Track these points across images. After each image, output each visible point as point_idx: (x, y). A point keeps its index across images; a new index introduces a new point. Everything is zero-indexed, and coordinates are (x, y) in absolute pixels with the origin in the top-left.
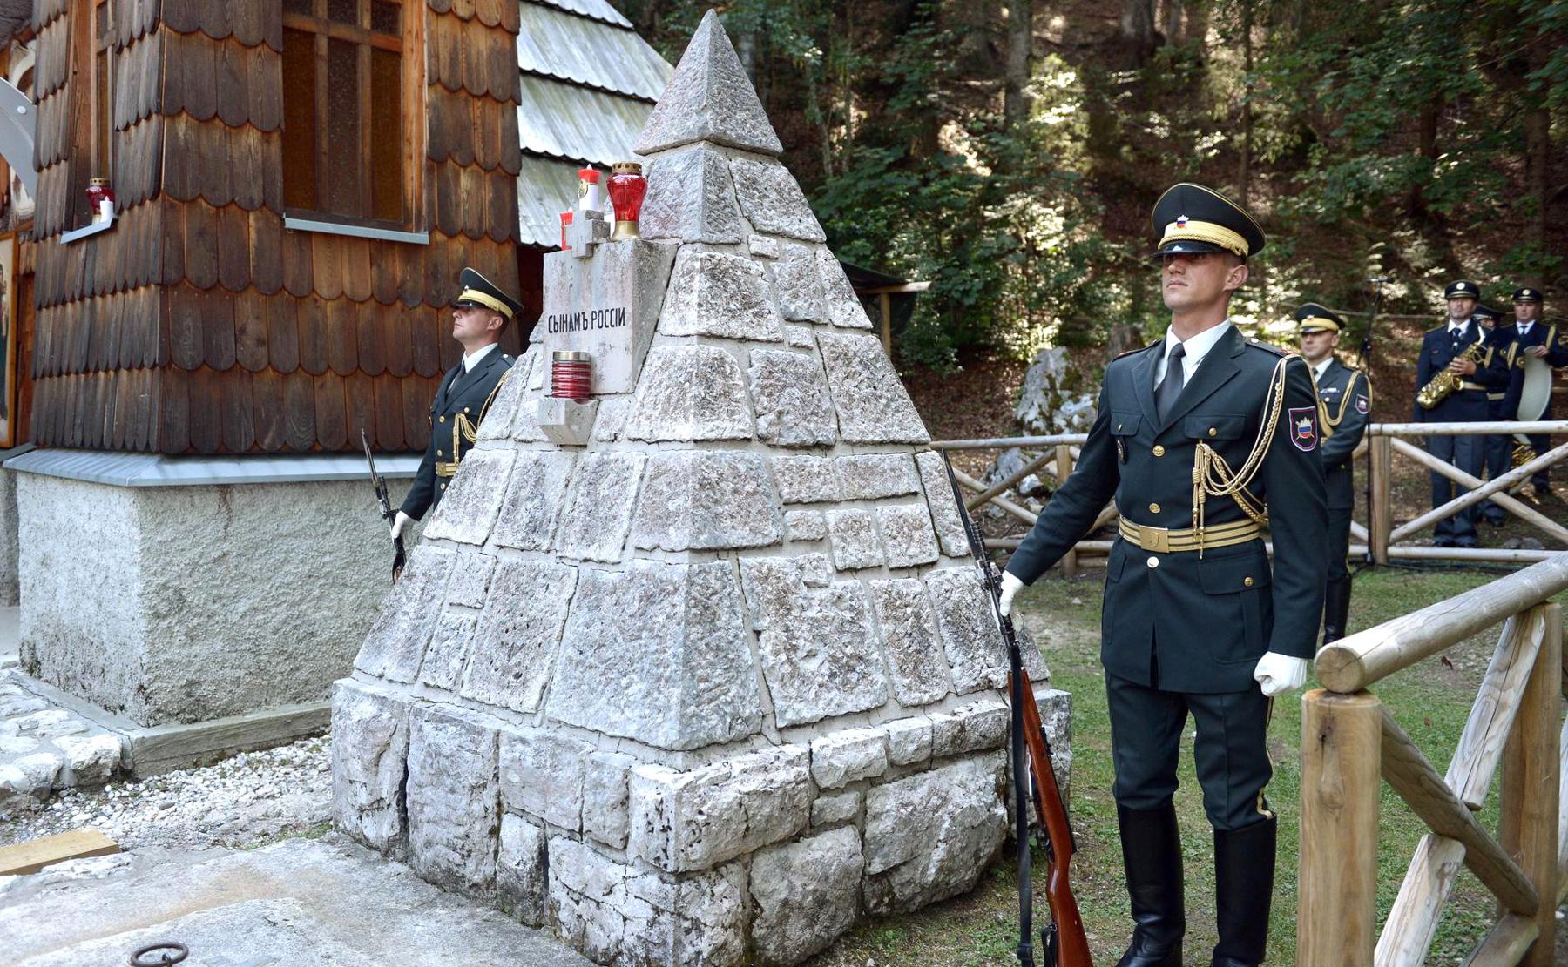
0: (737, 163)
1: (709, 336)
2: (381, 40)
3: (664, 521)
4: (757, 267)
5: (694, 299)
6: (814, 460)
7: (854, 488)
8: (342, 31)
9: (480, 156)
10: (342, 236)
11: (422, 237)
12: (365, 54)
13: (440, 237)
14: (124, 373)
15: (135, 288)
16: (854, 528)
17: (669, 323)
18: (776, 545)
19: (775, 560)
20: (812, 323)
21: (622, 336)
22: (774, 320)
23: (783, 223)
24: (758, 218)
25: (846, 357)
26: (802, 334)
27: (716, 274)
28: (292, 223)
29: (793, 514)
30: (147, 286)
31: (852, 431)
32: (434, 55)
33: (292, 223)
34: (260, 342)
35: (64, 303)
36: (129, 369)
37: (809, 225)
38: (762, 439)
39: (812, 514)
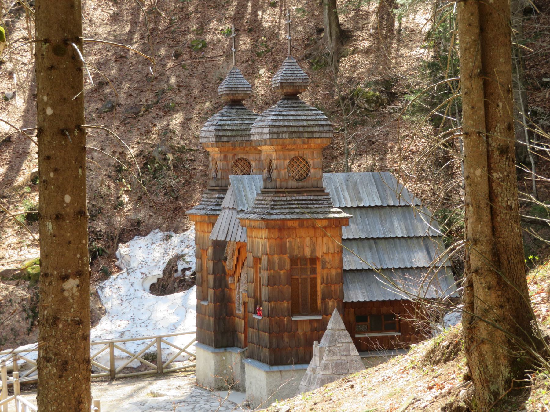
0: (337, 332)
1: (327, 360)
2: (312, 276)
8: (304, 276)
9: (334, 297)
10: (304, 320)
11: (320, 317)
12: (309, 280)
13: (325, 316)
21: (318, 359)
24: (339, 341)
25: (352, 360)
26: (344, 358)
27: (330, 351)
28: (294, 319)
32: (323, 278)
33: (294, 319)
34: (287, 343)
38: (334, 374)
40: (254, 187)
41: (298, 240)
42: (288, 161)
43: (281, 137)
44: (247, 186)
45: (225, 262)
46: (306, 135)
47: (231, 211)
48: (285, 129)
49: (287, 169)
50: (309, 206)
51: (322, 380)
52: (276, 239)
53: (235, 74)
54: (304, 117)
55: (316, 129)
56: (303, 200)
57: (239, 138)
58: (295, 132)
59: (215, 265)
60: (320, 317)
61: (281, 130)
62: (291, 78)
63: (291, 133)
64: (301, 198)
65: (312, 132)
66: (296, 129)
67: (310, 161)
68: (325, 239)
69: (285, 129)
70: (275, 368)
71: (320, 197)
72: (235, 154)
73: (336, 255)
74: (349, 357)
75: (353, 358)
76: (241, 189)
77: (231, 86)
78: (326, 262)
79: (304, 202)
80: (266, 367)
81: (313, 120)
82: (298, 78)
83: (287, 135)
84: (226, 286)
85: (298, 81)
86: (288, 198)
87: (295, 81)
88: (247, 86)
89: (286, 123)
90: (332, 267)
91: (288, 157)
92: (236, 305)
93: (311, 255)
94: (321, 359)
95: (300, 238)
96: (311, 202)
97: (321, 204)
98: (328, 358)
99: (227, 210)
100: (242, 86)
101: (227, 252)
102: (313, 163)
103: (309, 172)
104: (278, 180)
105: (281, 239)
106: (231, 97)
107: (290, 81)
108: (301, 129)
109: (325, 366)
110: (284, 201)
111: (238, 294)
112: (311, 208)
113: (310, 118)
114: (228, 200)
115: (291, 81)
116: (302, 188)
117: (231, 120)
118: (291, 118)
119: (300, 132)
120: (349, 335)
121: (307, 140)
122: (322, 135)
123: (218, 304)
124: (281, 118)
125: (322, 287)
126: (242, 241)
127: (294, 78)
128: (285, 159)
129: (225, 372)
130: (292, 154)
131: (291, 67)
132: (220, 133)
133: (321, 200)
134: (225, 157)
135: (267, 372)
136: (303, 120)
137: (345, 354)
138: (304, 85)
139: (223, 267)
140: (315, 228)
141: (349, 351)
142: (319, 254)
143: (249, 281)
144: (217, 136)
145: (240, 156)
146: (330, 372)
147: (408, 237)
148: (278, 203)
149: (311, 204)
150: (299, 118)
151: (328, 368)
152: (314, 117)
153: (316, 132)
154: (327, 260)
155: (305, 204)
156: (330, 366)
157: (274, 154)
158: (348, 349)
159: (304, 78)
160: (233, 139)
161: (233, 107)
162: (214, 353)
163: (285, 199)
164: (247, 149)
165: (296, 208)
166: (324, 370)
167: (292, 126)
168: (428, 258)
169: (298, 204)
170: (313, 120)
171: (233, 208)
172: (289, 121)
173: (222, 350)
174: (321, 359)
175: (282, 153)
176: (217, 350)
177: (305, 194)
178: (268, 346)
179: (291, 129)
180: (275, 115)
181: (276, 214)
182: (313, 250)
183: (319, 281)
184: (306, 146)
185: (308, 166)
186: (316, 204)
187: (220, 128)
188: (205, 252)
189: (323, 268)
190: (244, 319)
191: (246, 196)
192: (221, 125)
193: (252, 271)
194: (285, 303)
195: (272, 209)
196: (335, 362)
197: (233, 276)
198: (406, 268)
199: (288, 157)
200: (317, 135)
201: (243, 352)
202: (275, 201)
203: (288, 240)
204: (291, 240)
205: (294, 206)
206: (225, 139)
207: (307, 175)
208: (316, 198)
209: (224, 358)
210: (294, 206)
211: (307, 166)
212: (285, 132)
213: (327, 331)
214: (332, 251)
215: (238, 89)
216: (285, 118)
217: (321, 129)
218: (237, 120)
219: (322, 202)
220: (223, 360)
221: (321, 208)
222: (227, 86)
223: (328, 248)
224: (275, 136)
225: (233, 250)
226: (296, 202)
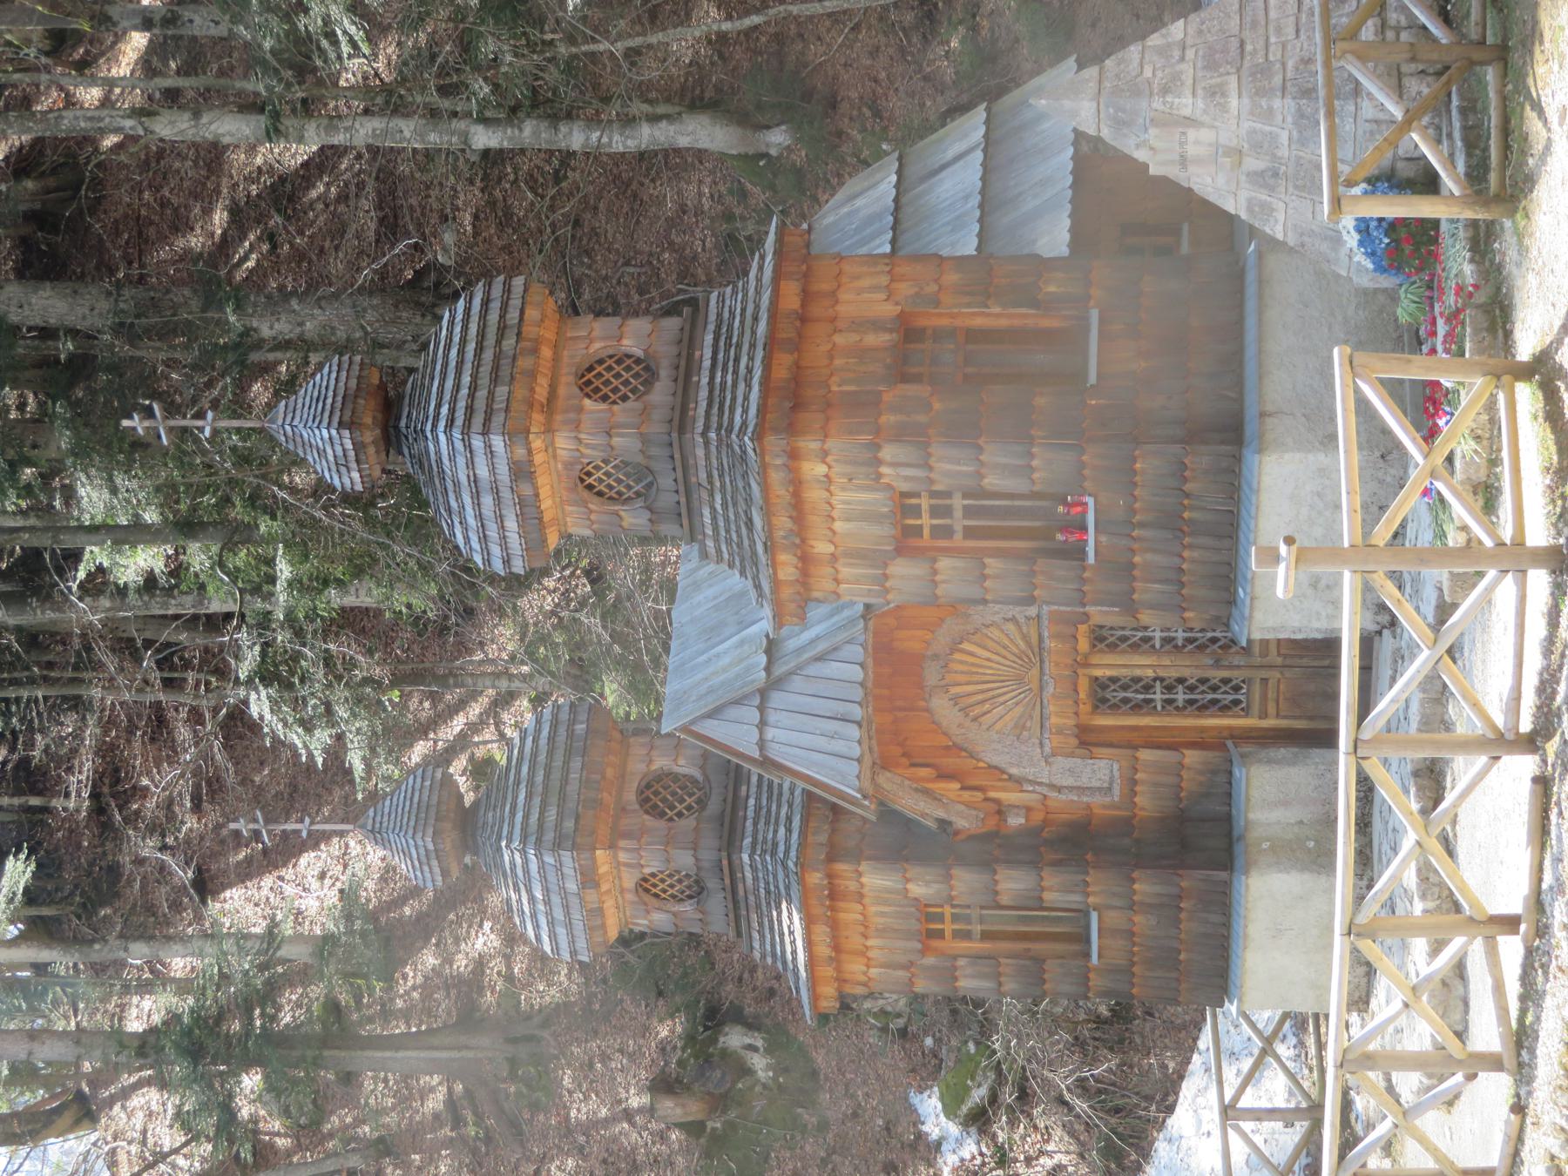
0: (1107, 84)
3: (1271, 110)
4: (1159, 74)
5: (1177, 101)
6: (1249, 48)
7: (1261, 31)
10: (1099, 356)
11: (1094, 315)
13: (1092, 303)
14: (1188, 487)
15: (1135, 472)
16: (1279, 30)
17: (1187, 112)
18: (1284, 65)
19: (1290, 64)
20: (1184, 49)
21: (1192, 134)
22: (1183, 66)
23: (1136, 63)
25: (1200, 32)
26: (1190, 54)
27: (1165, 91)
28: (1092, 378)
29: (1271, 58)
30: (1134, 460)
31: (1236, 31)
32: (969, 305)
33: (1092, 378)
35: (1133, 566)
36: (1185, 480)
37: (1134, 51)
39: (1272, 49)
40: (704, 657)
41: (838, 362)
42: (587, 402)
43: (503, 405)
44: (700, 676)
45: (957, 833)
46: (509, 343)
47: (772, 717)
48: (482, 394)
49: (614, 402)
50: (734, 340)
51: (1257, 94)
52: (828, 419)
53: (378, 819)
54: (454, 352)
55: (493, 317)
56: (714, 359)
57: (573, 788)
58: (496, 368)
59: (962, 861)
60: (1094, 315)
61: (480, 404)
62: (329, 401)
63: (495, 379)
64: (707, 363)
65: (502, 330)
66: (485, 370)
67: (597, 345)
68: (844, 296)
69: (482, 394)
70: (1250, 430)
71: (712, 317)
72: (624, 809)
73: (897, 270)
74: (1189, 41)
75: (1191, 31)
76: (703, 689)
77: (412, 823)
78: (917, 294)
79: (721, 356)
80: (1250, 458)
81: (465, 328)
82: (333, 382)
83: (501, 391)
84: (1032, 832)
85: (341, 384)
86: (703, 394)
87: (341, 392)
88: (419, 780)
89: (464, 392)
90: (936, 281)
91: (576, 402)
92: (1097, 800)
93: (891, 331)
94: (1190, 122)
95: (831, 358)
96: (723, 339)
97: (732, 314)
98: (1188, 92)
99: (770, 733)
100: (417, 794)
101: (923, 815)
102: (603, 338)
103: (629, 356)
104: (644, 429)
105: (829, 405)
106: (448, 825)
107: (339, 405)
108: (488, 355)
109: (1214, 94)
110: (710, 406)
111: (1059, 789)
112: (742, 334)
113: (456, 339)
114: (737, 734)
115: (339, 399)
116: (677, 368)
117: (513, 813)
118: (449, 383)
119: (497, 358)
120: (1120, 55)
121: (523, 344)
122: (515, 302)
123: (1089, 857)
124: (444, 410)
125: (997, 310)
126: (856, 652)
127: (331, 393)
128: (580, 410)
129: (1311, 844)
130: (567, 387)
131: (298, 413)
132: (549, 836)
133: (719, 315)
134: (626, 835)
135: (1260, 451)
136: (461, 352)
137: (1177, 54)
138: (356, 368)
139: (972, 838)
140: (804, 319)
141: (1169, 45)
142: (889, 310)
143: (973, 591)
144: (557, 845)
145: (631, 796)
146: (1233, 80)
147: (894, 228)
148: (714, 419)
149: (729, 338)
150: (452, 364)
151: (1221, 85)
152: (458, 329)
153: (502, 317)
154: (912, 291)
155: (727, 351)
156: (1213, 81)
157: (563, 442)
158: (1163, 51)
159: (335, 368)
160: (571, 805)
161: (480, 824)
162: (1247, 873)
163: (704, 404)
164: (610, 772)
165: (735, 372)
166: (1224, 95)
167: (475, 378)
168: (961, 163)
169: (725, 370)
170: (465, 328)
171: (762, 708)
172: (457, 387)
173: (1238, 849)
174: (1190, 122)
175: (558, 418)
176: (1239, 862)
177: (697, 353)
178: (1176, 449)
179: (484, 381)
180: (434, 426)
181: (745, 411)
182: (876, 325)
183: (979, 322)
184: (546, 352)
185: (611, 357)
186: (730, 327)
187: (533, 839)
188: (936, 943)
189: (938, 304)
190: (1136, 748)
191: (724, 670)
192: (524, 840)
193: (944, 563)
194: (1040, 401)
195: (730, 430)
196: (1200, 74)
197: (1001, 811)
198: (981, 206)
199: (576, 402)
200: (513, 316)
201: (1242, 756)
202: (707, 428)
203: (835, 388)
204: (834, 379)
205: (729, 378)
206: (569, 824)
207: (638, 361)
208: (711, 327)
209: (1265, 845)
210: (729, 378)
211: (609, 362)
212: (491, 395)
213: (1105, 133)
214: (884, 280)
215: (424, 804)
216: (447, 397)
217: (495, 306)
218: (515, 798)
219: (726, 309)
220: (1272, 848)
221: (743, 310)
222: (410, 832)
223: (875, 289)
224: (498, 419)
225: (916, 790)
226: (719, 374)
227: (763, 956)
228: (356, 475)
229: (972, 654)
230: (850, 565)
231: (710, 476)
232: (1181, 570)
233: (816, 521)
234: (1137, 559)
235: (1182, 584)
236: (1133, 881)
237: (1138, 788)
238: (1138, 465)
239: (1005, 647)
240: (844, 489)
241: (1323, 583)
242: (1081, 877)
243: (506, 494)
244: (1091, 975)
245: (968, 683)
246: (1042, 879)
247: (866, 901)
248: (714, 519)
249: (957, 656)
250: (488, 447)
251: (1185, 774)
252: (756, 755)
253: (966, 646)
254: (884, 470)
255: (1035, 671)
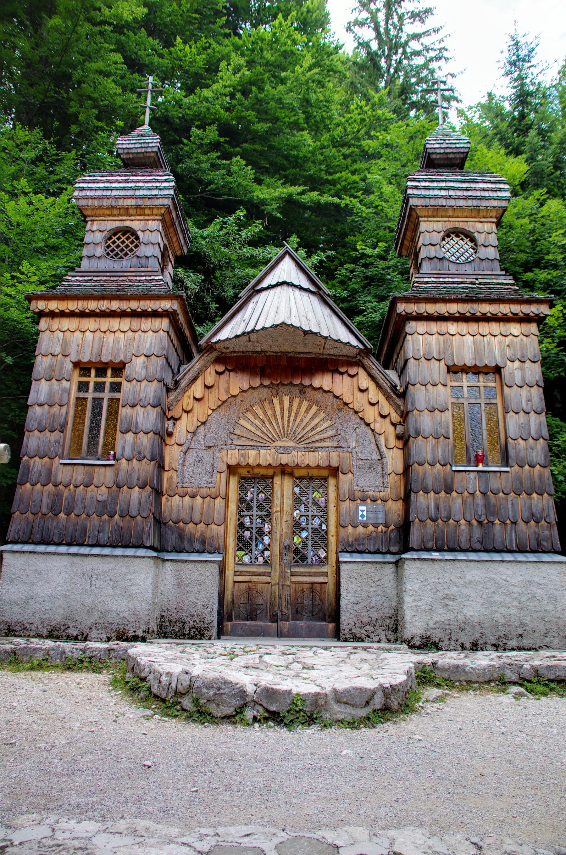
99: (297, 291)
227: (68, 281)
228: (437, 146)
229: (307, 411)
230: (438, 342)
231: (486, 283)
232: (449, 518)
233: (473, 327)
234: (454, 494)
235: (434, 520)
236: (142, 487)
237: (187, 498)
238: (535, 495)
239: (313, 429)
240: (500, 342)
241: (447, 601)
242: (148, 456)
243: (470, 193)
244: (46, 459)
245: (282, 409)
246: (146, 433)
247: (130, 334)
248: (453, 283)
249: (305, 404)
250: (500, 190)
251: (201, 526)
252: (259, 288)
253: (314, 408)
254: (517, 364)
255: (291, 444)
